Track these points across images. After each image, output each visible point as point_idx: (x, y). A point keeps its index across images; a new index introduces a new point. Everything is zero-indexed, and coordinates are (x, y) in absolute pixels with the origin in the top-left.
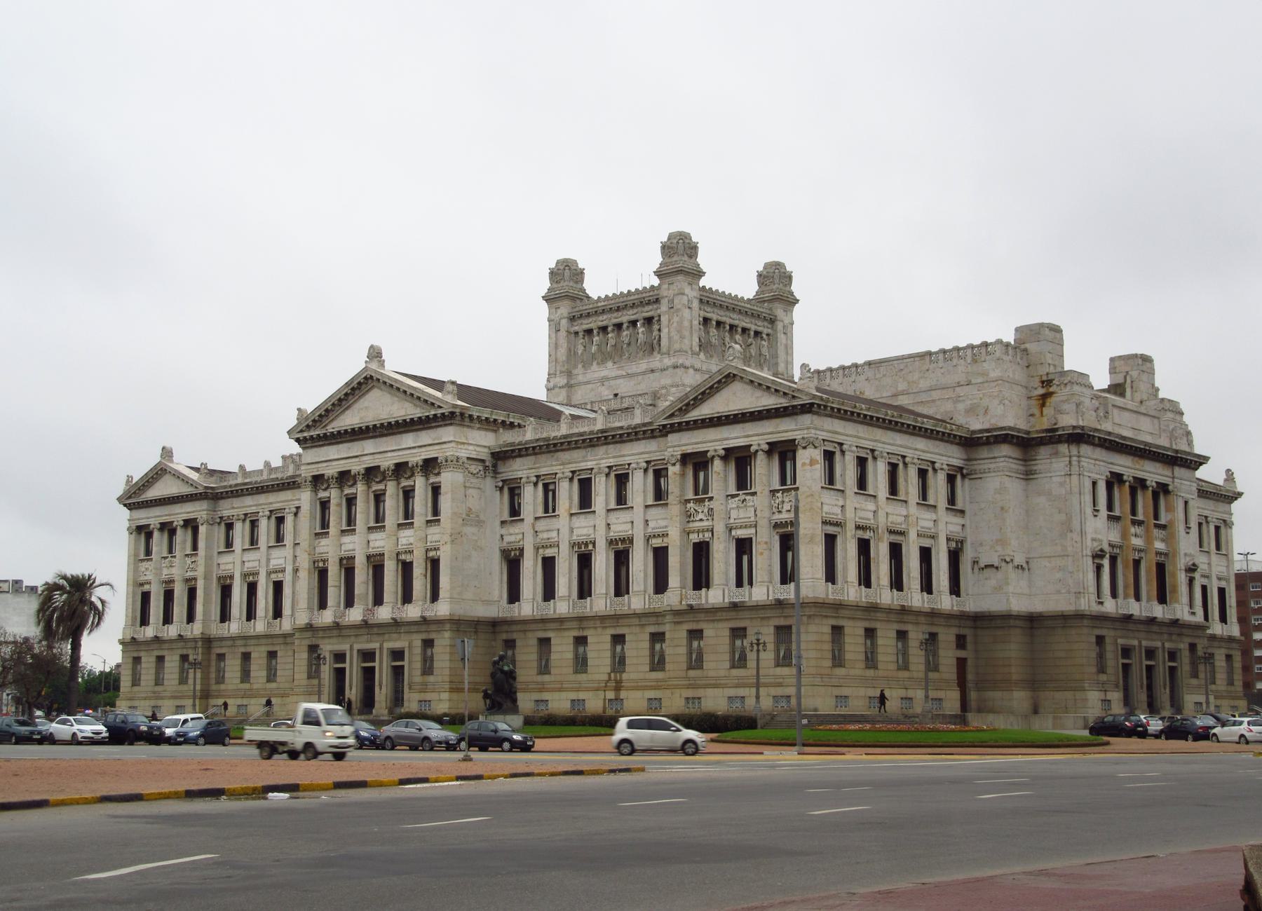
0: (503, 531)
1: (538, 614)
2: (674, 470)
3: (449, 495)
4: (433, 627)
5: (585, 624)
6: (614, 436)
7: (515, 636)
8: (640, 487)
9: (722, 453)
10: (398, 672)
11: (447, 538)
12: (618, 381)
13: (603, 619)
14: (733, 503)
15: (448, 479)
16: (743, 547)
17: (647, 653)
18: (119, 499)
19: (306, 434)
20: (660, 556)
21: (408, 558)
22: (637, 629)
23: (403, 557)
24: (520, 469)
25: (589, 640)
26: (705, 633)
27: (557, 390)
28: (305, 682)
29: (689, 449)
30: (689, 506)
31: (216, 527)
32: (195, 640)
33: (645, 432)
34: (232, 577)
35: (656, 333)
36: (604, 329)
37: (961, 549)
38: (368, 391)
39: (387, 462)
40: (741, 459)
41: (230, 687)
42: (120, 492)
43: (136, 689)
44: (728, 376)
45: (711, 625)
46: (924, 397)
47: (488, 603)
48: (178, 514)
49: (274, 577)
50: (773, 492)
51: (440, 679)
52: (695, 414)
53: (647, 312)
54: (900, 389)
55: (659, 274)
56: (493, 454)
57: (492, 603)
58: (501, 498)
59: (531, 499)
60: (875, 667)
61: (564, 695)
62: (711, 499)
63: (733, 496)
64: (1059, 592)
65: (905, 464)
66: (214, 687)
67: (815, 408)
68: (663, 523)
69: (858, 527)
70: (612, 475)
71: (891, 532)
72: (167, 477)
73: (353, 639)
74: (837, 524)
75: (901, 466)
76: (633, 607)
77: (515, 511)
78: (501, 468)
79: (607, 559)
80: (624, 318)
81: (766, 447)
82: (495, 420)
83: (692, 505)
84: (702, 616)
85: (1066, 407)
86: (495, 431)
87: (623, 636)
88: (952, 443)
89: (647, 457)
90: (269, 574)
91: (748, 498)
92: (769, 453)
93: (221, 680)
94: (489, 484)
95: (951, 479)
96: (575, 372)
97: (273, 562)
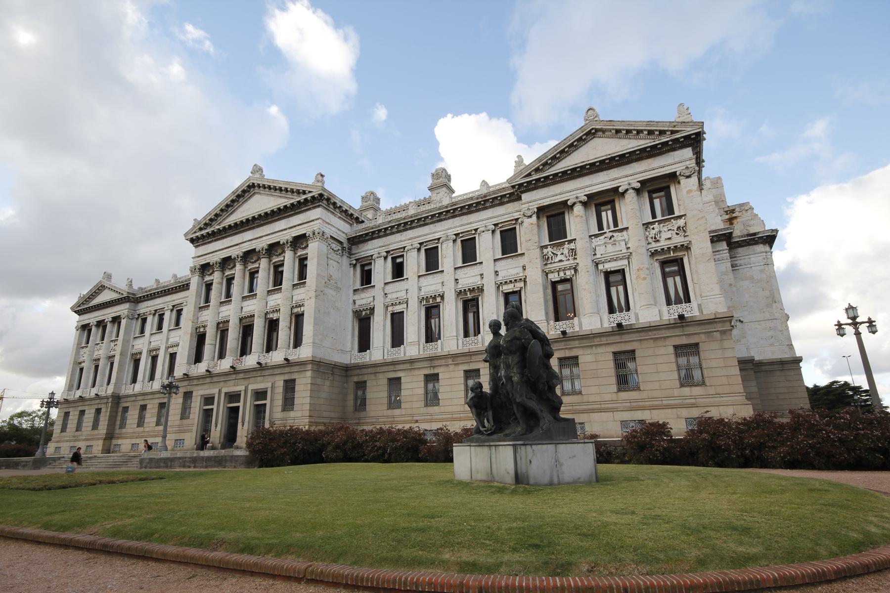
0: (356, 297)
1: (389, 358)
3: (315, 260)
4: (296, 369)
5: (437, 363)
7: (365, 378)
10: (260, 410)
11: (313, 294)
15: (313, 249)
21: (274, 316)
23: (271, 316)
24: (372, 248)
26: (580, 360)
28: (178, 423)
29: (547, 202)
30: (545, 251)
31: (135, 321)
32: (107, 398)
34: (141, 353)
40: (605, 201)
41: (129, 431)
43: (63, 434)
44: (589, 133)
45: (589, 351)
47: (343, 352)
48: (107, 314)
49: (171, 350)
50: (646, 225)
51: (299, 414)
55: (431, 189)
56: (349, 239)
57: (346, 351)
58: (354, 274)
59: (381, 271)
63: (596, 236)
64: (772, 345)
66: (117, 431)
70: (459, 241)
72: (106, 290)
73: (222, 384)
77: (367, 278)
78: (353, 252)
81: (638, 185)
82: (352, 215)
83: (549, 249)
84: (576, 343)
86: (351, 225)
89: (495, 221)
90: (167, 348)
91: (614, 234)
93: (123, 425)
94: (345, 261)
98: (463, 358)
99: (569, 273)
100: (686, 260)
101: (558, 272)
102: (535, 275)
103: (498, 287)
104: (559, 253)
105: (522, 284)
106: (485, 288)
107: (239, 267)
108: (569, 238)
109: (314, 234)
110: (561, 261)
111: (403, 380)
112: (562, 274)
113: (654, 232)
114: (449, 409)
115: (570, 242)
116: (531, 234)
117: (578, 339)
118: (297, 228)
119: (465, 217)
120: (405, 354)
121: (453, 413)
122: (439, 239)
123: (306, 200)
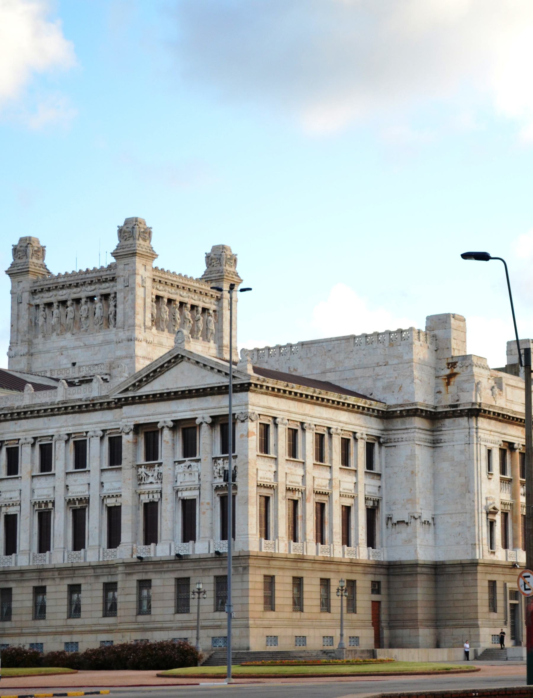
2: (127, 439)
5: (45, 575)
6: (73, 407)
8: (97, 453)
12: (76, 352)
13: (61, 571)
14: (180, 468)
16: (189, 508)
17: (101, 600)
20: (114, 515)
22: (92, 580)
25: (48, 589)
26: (153, 583)
27: (18, 358)
29: (142, 421)
30: (140, 470)
33: (101, 404)
35: (112, 308)
36: (63, 303)
37: (377, 507)
40: (187, 430)
44: (176, 357)
45: (158, 576)
46: (348, 375)
50: (215, 459)
52: (146, 390)
53: (105, 288)
54: (328, 367)
55: (115, 254)
60: (302, 610)
62: (160, 464)
63: (180, 462)
65: (330, 435)
67: (252, 387)
68: (116, 485)
69: (288, 490)
70: (71, 442)
71: (317, 493)
74: (270, 487)
75: (326, 436)
76: (88, 560)
79: (66, 517)
80: (83, 293)
81: (209, 420)
83: (142, 470)
85: (466, 386)
87: (79, 586)
88: (371, 416)
91: (193, 464)
92: (212, 425)
95: (370, 448)
96: (35, 341)
98: (68, 572)
99: (157, 496)
101: (148, 493)
103: (103, 500)
104: (150, 475)
108: (159, 461)
110: (151, 483)
111: (14, 591)
114: (53, 623)
117: (152, 564)
119: (77, 416)
120: (16, 564)
121: (56, 627)
122: (52, 436)
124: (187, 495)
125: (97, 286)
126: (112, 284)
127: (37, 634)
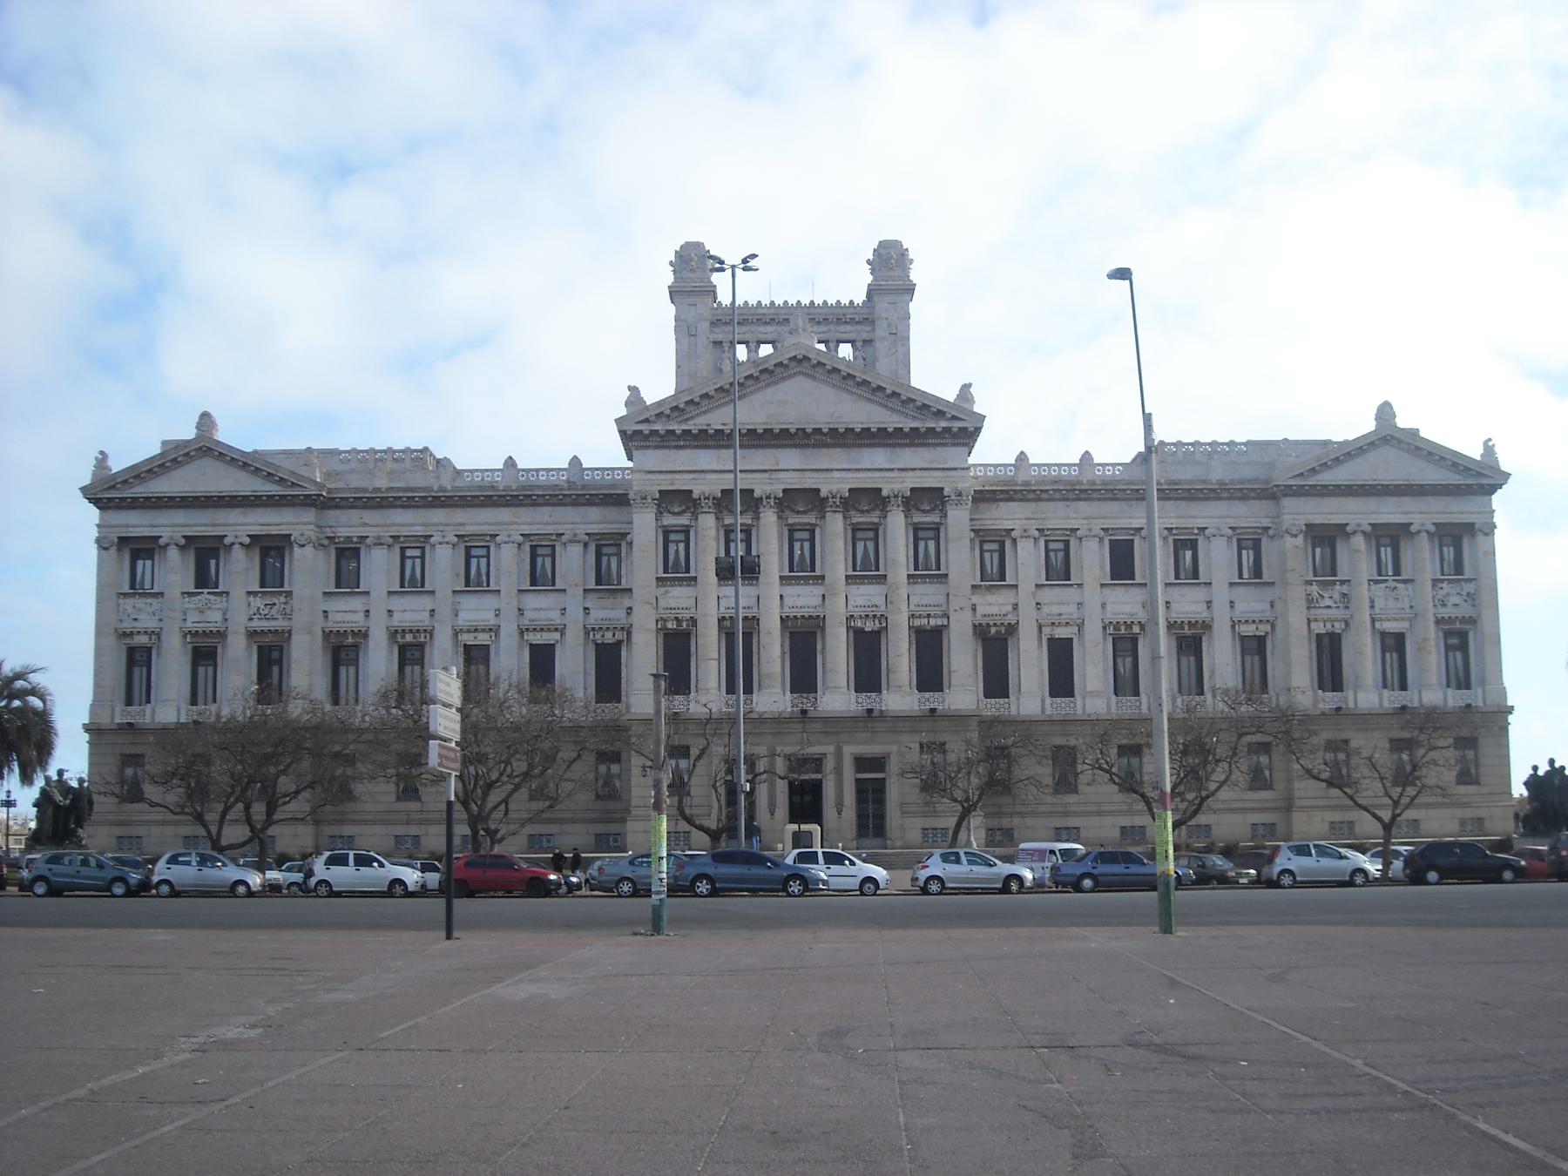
0: (975, 599)
9: (1369, 529)
18: (84, 490)
19: (657, 427)
21: (869, 626)
24: (1006, 516)
29: (1318, 520)
31: (321, 553)
38: (784, 379)
39: (835, 484)
40: (1390, 537)
42: (87, 481)
48: (239, 525)
49: (468, 639)
52: (1326, 478)
59: (1027, 561)
61: (1108, 820)
83: (1315, 587)
97: (462, 615)
99: (1339, 627)
100: (1471, 635)
102: (1296, 618)
105: (1269, 628)
106: (1215, 625)
107: (769, 517)
109: (960, 495)
112: (1329, 626)
113: (1442, 593)
115: (1343, 582)
116: (1290, 555)
118: (918, 473)
119: (1184, 503)
123: (947, 430)
124: (1390, 626)
125: (832, 328)
126: (859, 327)
127: (1066, 814)
